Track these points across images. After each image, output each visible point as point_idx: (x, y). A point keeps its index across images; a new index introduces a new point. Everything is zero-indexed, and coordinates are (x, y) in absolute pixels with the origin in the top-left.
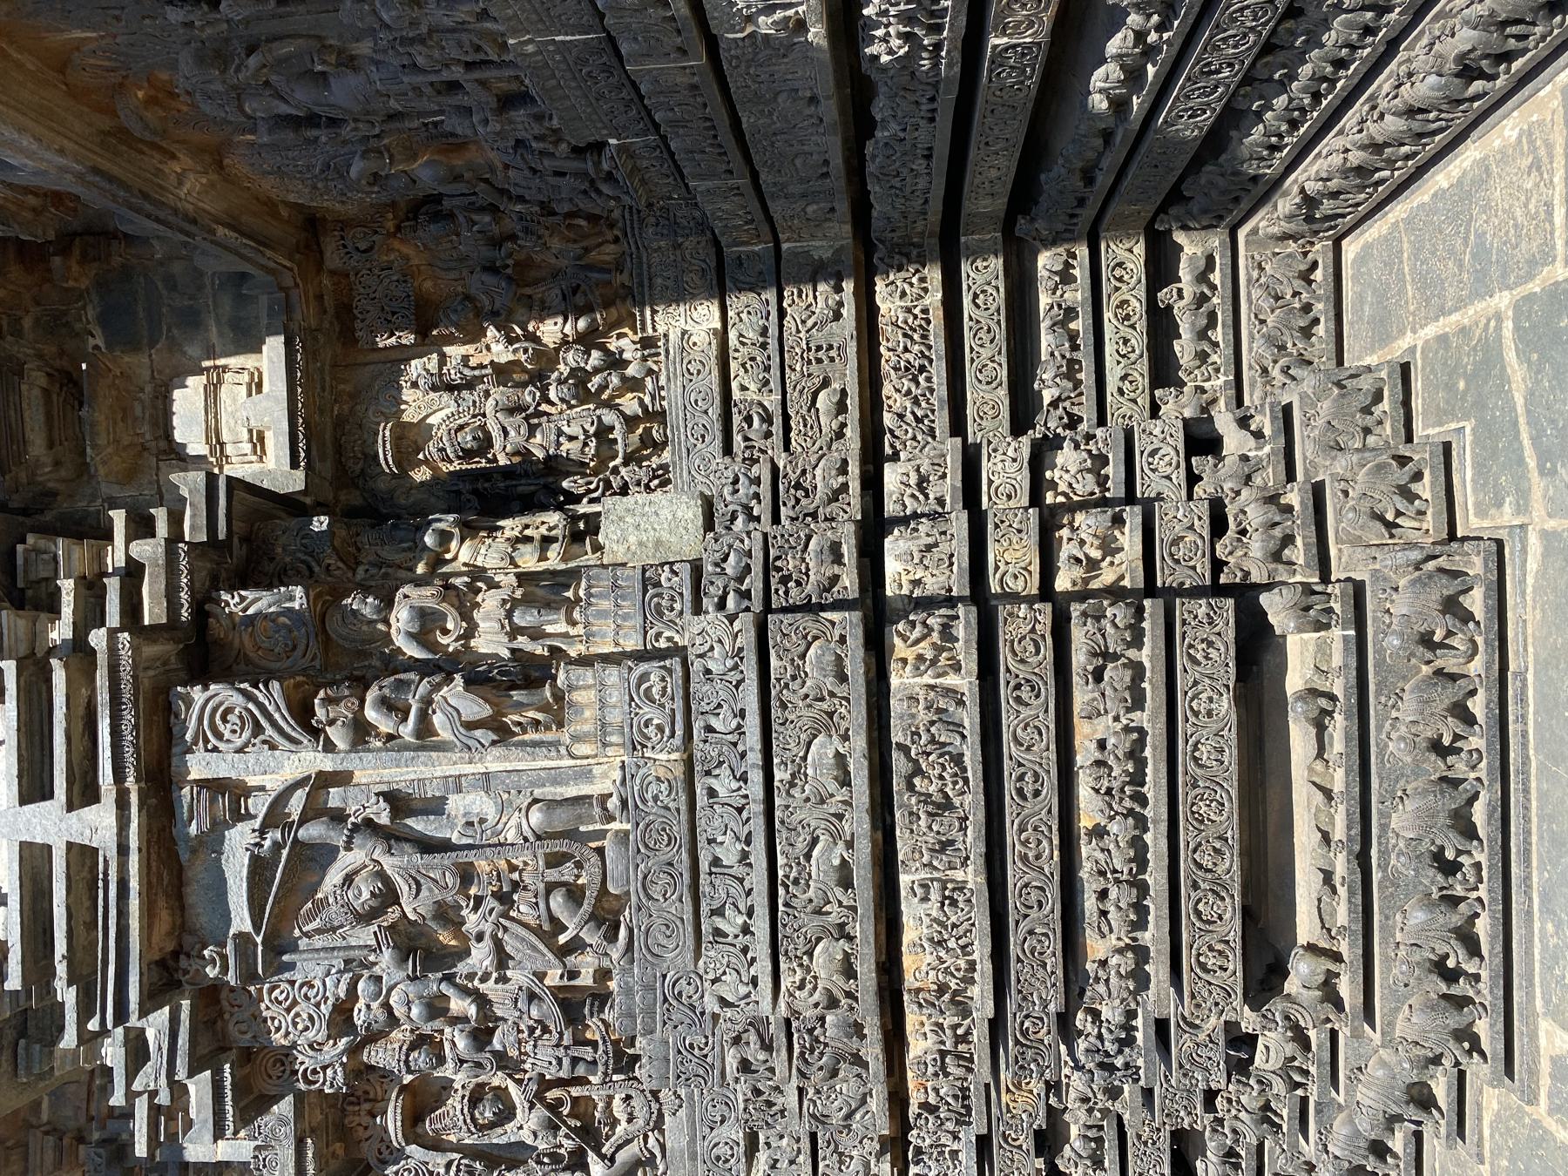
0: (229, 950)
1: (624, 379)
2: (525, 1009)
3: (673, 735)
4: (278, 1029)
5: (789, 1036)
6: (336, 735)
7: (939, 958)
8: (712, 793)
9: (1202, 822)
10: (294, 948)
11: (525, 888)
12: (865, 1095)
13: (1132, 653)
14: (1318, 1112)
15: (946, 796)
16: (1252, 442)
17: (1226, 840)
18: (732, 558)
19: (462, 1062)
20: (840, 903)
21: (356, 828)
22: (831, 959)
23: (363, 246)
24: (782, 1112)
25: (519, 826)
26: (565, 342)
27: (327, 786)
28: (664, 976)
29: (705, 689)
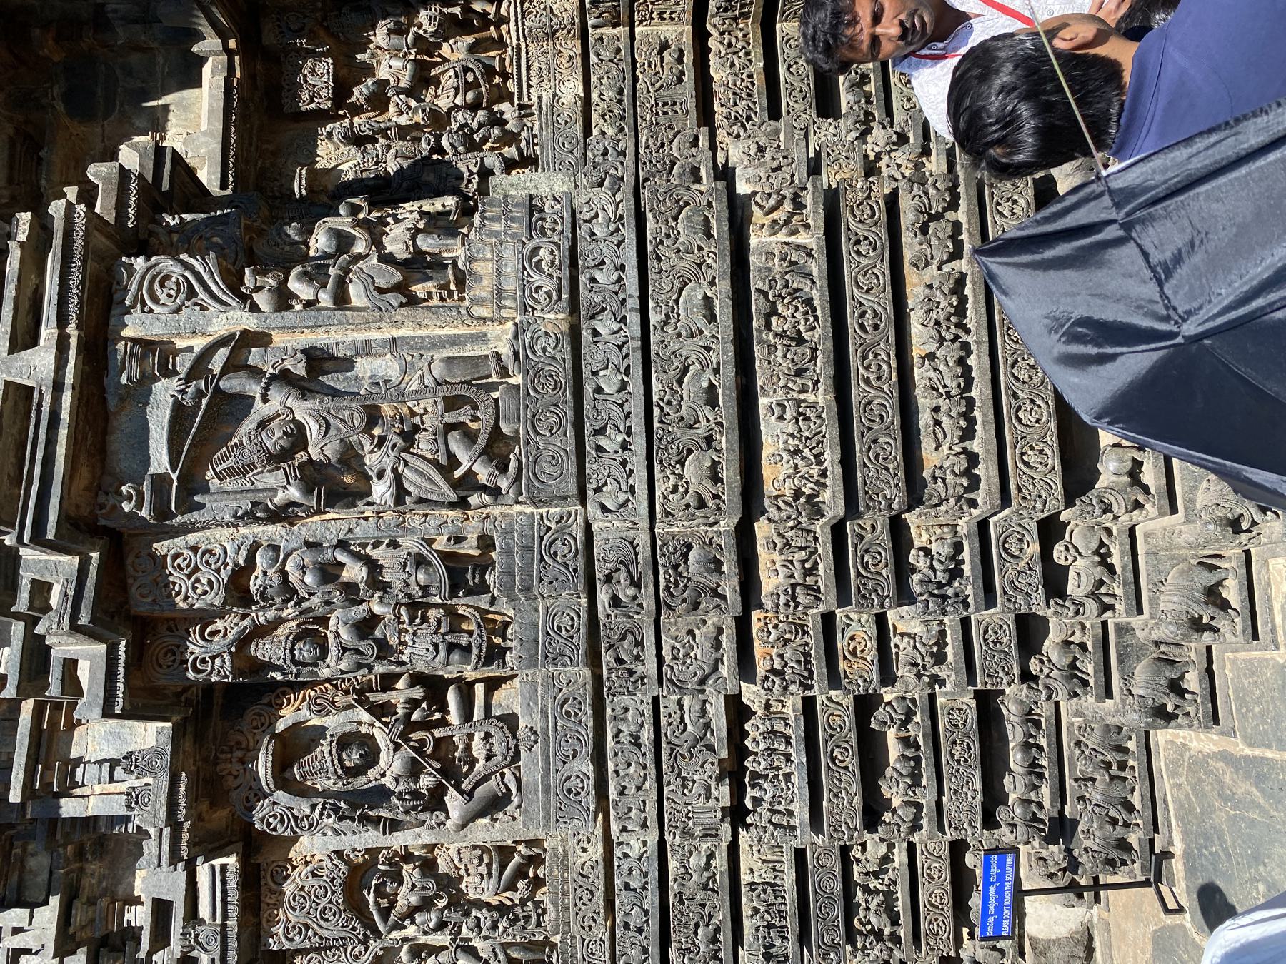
0: (146, 488)
3: (560, 298)
4: (178, 593)
6: (262, 299)
7: (796, 466)
8: (595, 333)
9: (1017, 342)
10: (206, 490)
11: (425, 430)
13: (950, 215)
14: (1121, 661)
15: (799, 332)
18: (606, 183)
19: (345, 650)
20: (708, 420)
21: (273, 378)
24: (643, 678)
26: (456, 107)
27: (249, 346)
28: (542, 538)
29: (591, 247)
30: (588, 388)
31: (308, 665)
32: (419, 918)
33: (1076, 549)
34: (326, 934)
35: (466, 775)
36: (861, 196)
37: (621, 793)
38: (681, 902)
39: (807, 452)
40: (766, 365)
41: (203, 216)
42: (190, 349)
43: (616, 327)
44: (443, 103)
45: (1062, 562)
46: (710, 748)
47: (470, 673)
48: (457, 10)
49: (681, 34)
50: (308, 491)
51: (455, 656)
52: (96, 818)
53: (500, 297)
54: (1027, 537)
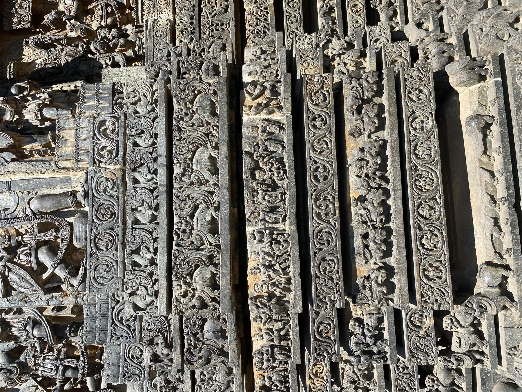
2: (30, 330)
3: (117, 154)
5: (182, 338)
7: (269, 276)
8: (136, 181)
9: (421, 190)
11: (26, 245)
12: (229, 382)
13: (377, 100)
14: (483, 384)
16: (424, 34)
17: (436, 200)
20: (210, 244)
22: (204, 278)
26: (101, 27)
28: (113, 308)
29: (134, 122)
33: (458, 321)
36: (317, 87)
39: (277, 267)
40: (251, 204)
43: (149, 177)
44: (94, 25)
45: (449, 329)
54: (426, 313)
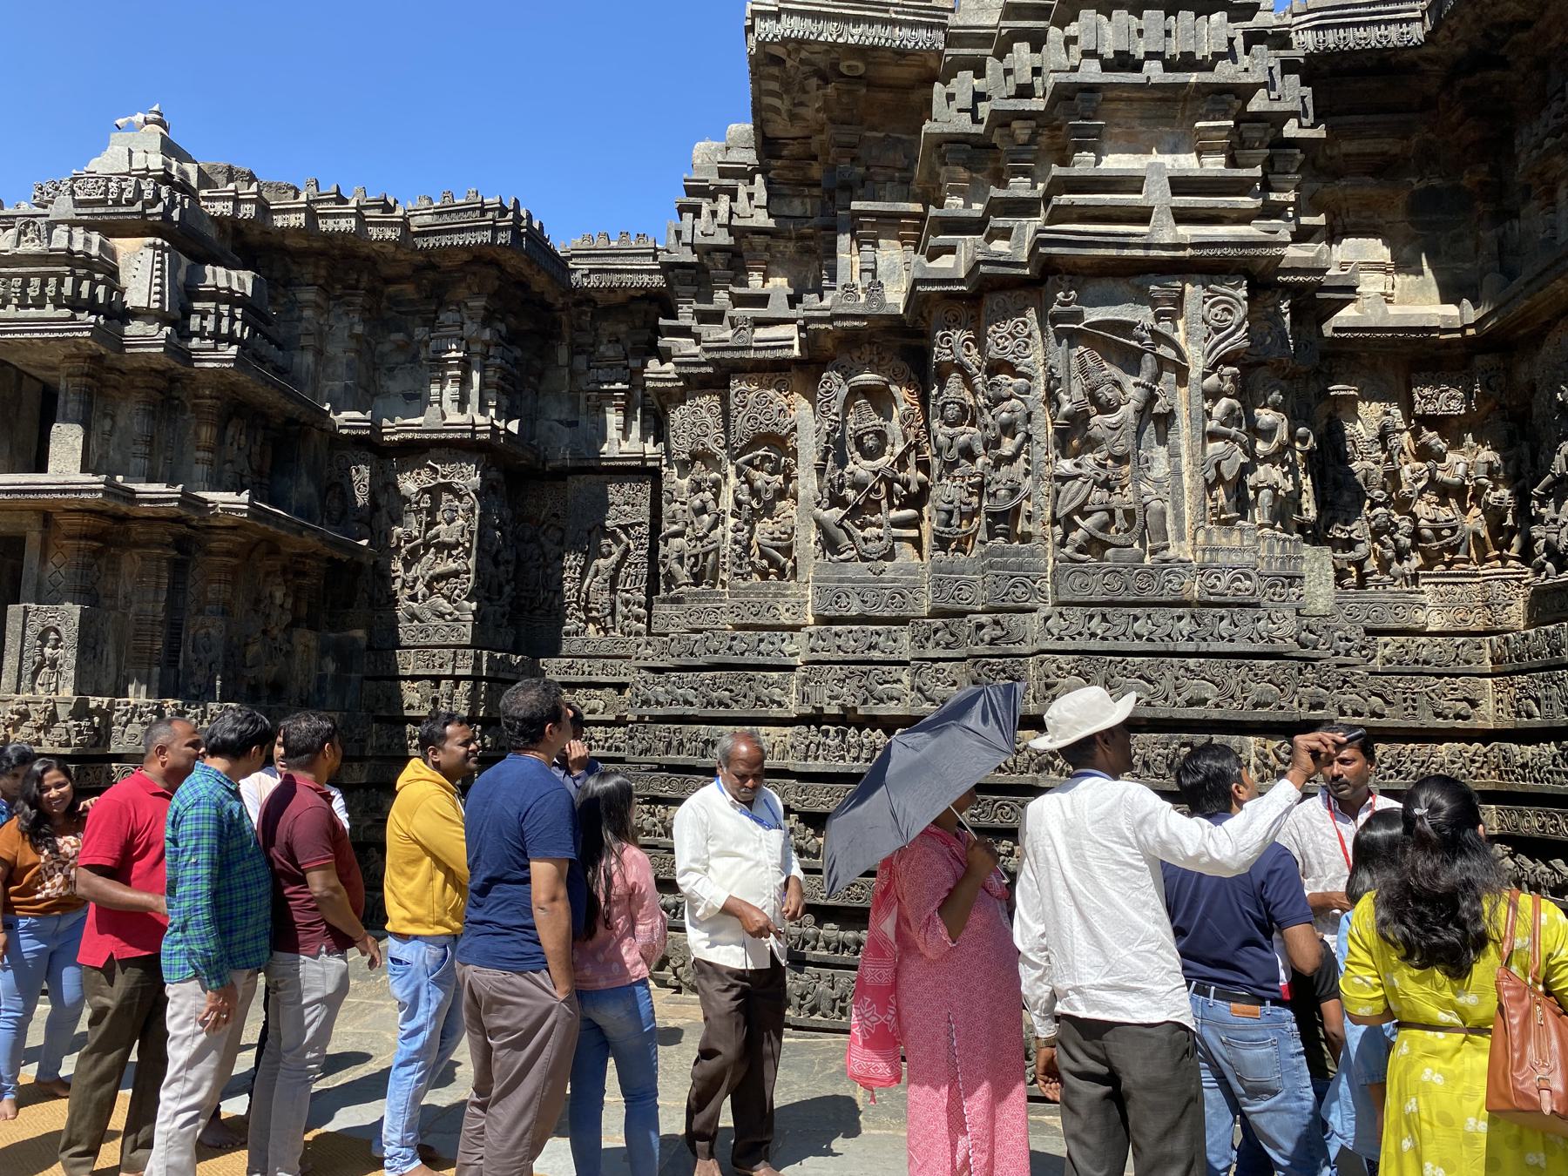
1: (1390, 561)
3: (1210, 594)
4: (998, 327)
6: (1213, 379)
8: (1180, 618)
10: (1071, 346)
19: (952, 439)
21: (1152, 390)
23: (1492, 383)
25: (1151, 494)
26: (1415, 519)
30: (1138, 611)
31: (942, 412)
32: (745, 487)
34: (739, 420)
35: (853, 523)
37: (836, 634)
38: (749, 680)
41: (1288, 327)
42: (1176, 330)
43: (1185, 633)
46: (865, 702)
47: (925, 526)
48: (1509, 522)
49: (1485, 719)
50: (1066, 417)
51: (943, 516)
52: (835, 257)
53: (1212, 550)
